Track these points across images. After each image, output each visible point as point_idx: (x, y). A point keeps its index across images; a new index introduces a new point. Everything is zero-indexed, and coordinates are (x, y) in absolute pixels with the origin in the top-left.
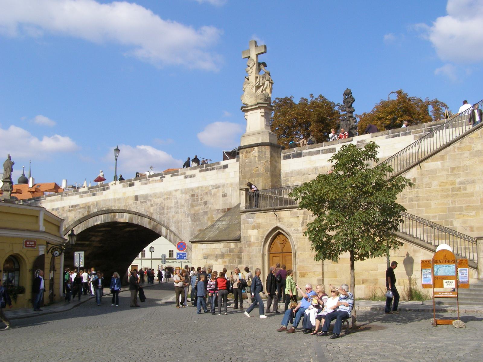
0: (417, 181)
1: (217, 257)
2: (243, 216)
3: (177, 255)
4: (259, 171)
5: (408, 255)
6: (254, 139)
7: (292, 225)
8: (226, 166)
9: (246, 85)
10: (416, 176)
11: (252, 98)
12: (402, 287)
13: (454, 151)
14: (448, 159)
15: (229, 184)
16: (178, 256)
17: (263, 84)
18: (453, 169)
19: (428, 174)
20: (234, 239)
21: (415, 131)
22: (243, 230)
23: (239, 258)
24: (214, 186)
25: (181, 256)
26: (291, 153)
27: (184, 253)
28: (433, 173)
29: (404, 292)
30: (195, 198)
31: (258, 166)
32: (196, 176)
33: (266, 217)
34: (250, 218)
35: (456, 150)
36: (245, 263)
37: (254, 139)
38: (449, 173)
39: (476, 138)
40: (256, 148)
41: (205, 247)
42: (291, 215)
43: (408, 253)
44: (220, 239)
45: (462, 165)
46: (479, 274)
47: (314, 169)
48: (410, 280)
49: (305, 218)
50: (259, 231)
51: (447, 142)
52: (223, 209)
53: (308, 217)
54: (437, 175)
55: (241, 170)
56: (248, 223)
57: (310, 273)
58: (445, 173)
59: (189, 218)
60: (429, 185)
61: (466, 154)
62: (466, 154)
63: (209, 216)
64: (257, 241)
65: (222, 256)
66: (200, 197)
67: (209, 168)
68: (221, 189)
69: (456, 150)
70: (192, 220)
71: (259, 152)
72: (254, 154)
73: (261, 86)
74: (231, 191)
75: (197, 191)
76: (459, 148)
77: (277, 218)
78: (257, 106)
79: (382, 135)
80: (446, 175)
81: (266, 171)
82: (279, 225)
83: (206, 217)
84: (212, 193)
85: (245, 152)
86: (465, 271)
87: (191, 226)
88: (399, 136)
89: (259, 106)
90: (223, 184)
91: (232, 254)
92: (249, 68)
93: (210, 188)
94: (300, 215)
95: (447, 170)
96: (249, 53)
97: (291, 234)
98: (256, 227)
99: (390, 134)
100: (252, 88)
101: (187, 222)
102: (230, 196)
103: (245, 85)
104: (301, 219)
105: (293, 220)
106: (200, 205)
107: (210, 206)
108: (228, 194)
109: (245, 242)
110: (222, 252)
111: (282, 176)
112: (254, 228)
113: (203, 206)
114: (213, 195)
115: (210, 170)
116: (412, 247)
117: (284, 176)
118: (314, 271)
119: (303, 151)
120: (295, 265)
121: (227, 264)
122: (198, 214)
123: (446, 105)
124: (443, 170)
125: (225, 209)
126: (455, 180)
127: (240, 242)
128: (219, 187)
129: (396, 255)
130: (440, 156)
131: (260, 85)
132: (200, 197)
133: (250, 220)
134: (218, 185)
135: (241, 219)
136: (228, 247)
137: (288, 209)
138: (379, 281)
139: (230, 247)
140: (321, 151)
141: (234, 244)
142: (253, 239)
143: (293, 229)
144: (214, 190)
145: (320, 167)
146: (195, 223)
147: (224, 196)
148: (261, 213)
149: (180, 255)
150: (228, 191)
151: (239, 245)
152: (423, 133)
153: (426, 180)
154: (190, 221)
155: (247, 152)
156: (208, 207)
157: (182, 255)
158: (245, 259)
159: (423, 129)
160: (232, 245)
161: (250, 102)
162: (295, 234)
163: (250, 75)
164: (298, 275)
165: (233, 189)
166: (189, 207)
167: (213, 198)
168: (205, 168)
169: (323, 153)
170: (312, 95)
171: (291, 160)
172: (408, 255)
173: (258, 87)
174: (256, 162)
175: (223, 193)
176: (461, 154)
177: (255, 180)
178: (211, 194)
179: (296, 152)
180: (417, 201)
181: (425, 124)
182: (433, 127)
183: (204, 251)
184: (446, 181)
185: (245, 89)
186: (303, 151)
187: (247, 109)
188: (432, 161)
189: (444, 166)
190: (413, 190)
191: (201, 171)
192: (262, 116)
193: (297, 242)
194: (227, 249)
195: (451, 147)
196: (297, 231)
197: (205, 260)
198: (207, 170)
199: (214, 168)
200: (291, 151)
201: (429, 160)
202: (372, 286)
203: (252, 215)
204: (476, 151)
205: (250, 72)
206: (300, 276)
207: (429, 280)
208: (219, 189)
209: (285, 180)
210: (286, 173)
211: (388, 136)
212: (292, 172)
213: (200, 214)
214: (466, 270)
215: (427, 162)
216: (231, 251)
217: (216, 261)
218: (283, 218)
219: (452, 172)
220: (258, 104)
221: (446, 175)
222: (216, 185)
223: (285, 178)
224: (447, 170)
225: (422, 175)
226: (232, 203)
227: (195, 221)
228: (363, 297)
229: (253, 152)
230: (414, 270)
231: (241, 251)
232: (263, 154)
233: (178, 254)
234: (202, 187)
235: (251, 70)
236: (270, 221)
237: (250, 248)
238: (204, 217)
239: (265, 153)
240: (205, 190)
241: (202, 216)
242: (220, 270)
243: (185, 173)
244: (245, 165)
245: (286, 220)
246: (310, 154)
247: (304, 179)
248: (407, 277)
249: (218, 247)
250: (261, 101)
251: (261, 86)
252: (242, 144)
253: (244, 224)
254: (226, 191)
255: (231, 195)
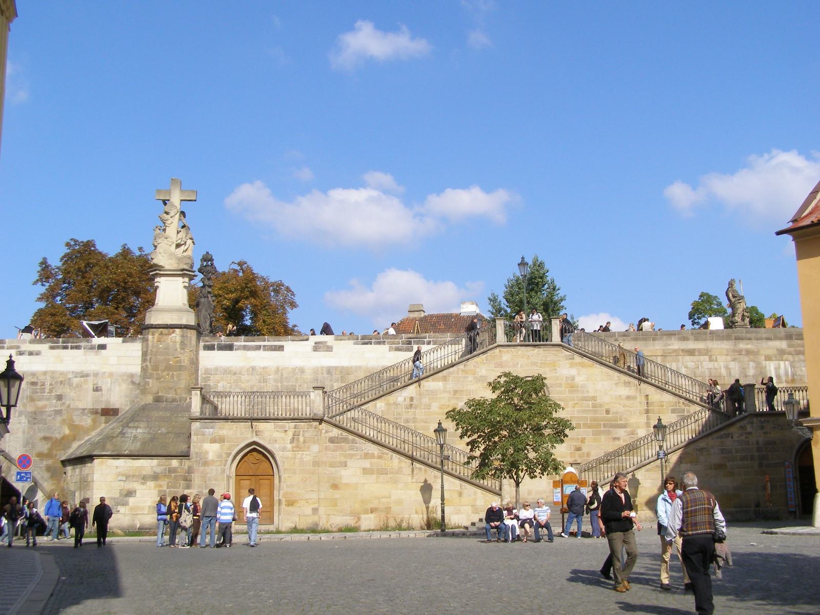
0: (414, 401)
1: (144, 479)
2: (196, 426)
3: (17, 476)
4: (181, 363)
5: (426, 481)
6: (174, 317)
7: (276, 441)
8: (102, 347)
9: (162, 239)
10: (414, 395)
11: (172, 259)
12: (420, 515)
13: (458, 374)
14: (450, 381)
15: (106, 374)
16: (19, 476)
17: (185, 243)
18: (456, 392)
19: (428, 395)
20: (178, 454)
21: (391, 341)
22: (195, 442)
23: (186, 480)
24: (77, 373)
25: (23, 477)
26: (216, 343)
27: (28, 473)
28: (433, 393)
29: (422, 521)
30: (39, 387)
31: (179, 356)
32: (43, 353)
33: (235, 429)
34: (208, 429)
35: (460, 372)
36: (196, 488)
37: (174, 317)
38: (451, 395)
39: (481, 363)
40: (178, 330)
41: (123, 464)
42: (275, 428)
43: (426, 479)
44: (153, 453)
45: (465, 389)
46: (502, 500)
47: (251, 369)
48: (427, 508)
49: (297, 433)
50: (222, 446)
51: (449, 363)
52: (93, 409)
53: (301, 433)
54: (439, 396)
55: (151, 358)
56: (204, 435)
57: (301, 501)
58: (447, 395)
59: (23, 417)
60: (428, 407)
61: (470, 378)
62: (470, 378)
63: (65, 417)
64: (219, 458)
65: (155, 477)
66: (48, 387)
67: (70, 345)
68: (90, 379)
69: (460, 372)
70: (29, 422)
71: (182, 336)
72: (174, 338)
73: (183, 244)
74: (111, 383)
75: (42, 378)
76: (463, 371)
77: (252, 431)
78: (181, 273)
79: (349, 339)
80: (448, 397)
81: (190, 364)
82: (256, 439)
83: (59, 418)
84: (74, 384)
85: (159, 333)
86: (585, 491)
87: (26, 431)
88: (371, 344)
89: (188, 273)
90: (95, 372)
91: (173, 475)
92: (168, 217)
93: (70, 376)
94: (289, 429)
95: (449, 392)
96: (170, 195)
97: (275, 451)
98: (221, 440)
99: (359, 340)
100: (170, 245)
101: (19, 423)
102: (108, 391)
103: (160, 238)
104: (290, 434)
105: (277, 435)
106: (48, 399)
107: (68, 403)
108: (104, 388)
109: (199, 459)
110: (155, 472)
111: (199, 372)
112: (213, 441)
113: (55, 401)
114: (74, 385)
115: (71, 349)
116: (433, 473)
117: (204, 372)
118: (307, 498)
119: (235, 343)
120: (278, 492)
121: (165, 488)
122: (42, 412)
123: (291, 291)
124: (444, 392)
125: (97, 409)
126: (457, 404)
127: (189, 459)
128: (87, 375)
129: (414, 480)
130: (443, 376)
131: (182, 243)
132: (48, 388)
133: (206, 430)
134: (85, 372)
135: (192, 428)
136: (166, 466)
137: (272, 421)
138: (392, 509)
139: (170, 465)
140: (262, 347)
141: (178, 462)
142: (211, 456)
143: (277, 446)
144: (78, 379)
145: (261, 368)
146: (36, 427)
147: (97, 389)
148: (227, 422)
149: (22, 475)
150: (105, 384)
151: (186, 463)
152: (401, 345)
153: (425, 400)
154: (24, 423)
155: (161, 334)
156: (64, 404)
157: (24, 475)
158: (196, 482)
159: (401, 340)
160: (175, 463)
161: (168, 265)
162: (281, 453)
163: (168, 225)
164: (284, 503)
165: (113, 380)
166: (25, 401)
167: (74, 392)
168: (61, 344)
169: (264, 350)
170: (140, 249)
171: (216, 353)
172: (426, 481)
173: (178, 246)
174: (176, 350)
175: (94, 385)
176: (465, 378)
177: (173, 374)
178: (70, 385)
179: (223, 342)
180: (414, 423)
181: (403, 335)
182: (412, 340)
183: (119, 470)
184: (448, 403)
185: (158, 244)
186: (235, 343)
187: (162, 273)
188: (433, 381)
189: (445, 388)
190: (409, 410)
191: (52, 348)
192: (185, 287)
193: (284, 462)
194: (165, 467)
195: (455, 368)
196: (284, 449)
197: (122, 483)
198: (65, 348)
199: (80, 346)
200: (216, 341)
201: (430, 379)
202: (383, 515)
203: (211, 425)
204: (480, 376)
205: (169, 222)
206: (286, 505)
207: (559, 498)
208: (88, 378)
209: (205, 378)
210: (207, 368)
211: (356, 342)
212: (216, 369)
213: (47, 413)
214: (585, 489)
215: (427, 381)
216: (172, 470)
217: (143, 484)
218: (262, 432)
219: (454, 394)
220: (182, 270)
221: (448, 397)
222: (82, 372)
223: (204, 376)
224: (449, 392)
225: (420, 394)
226: (112, 403)
227: (35, 424)
228: (372, 528)
229: (173, 335)
230: (432, 497)
231: (190, 471)
232: (189, 341)
233: (18, 473)
234: (53, 372)
235: (171, 219)
236: (242, 434)
237: (206, 467)
238: (53, 419)
239: (191, 339)
240: (58, 378)
241: (50, 416)
242: (526, 482)
243: (18, 347)
244: (157, 351)
245: (267, 434)
246: (245, 348)
247: (234, 380)
248: (424, 506)
249: (148, 465)
250: (186, 267)
251: (183, 244)
252: (152, 320)
253: (196, 434)
254: (100, 383)
255: (110, 390)
